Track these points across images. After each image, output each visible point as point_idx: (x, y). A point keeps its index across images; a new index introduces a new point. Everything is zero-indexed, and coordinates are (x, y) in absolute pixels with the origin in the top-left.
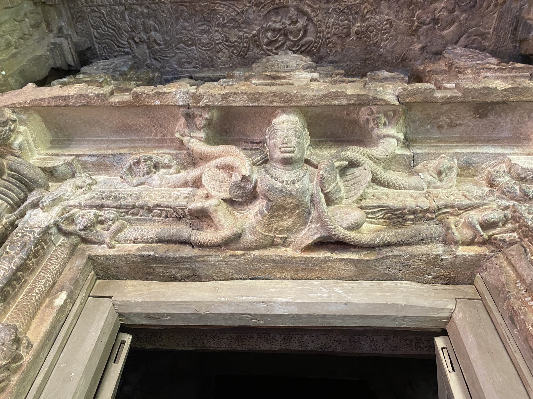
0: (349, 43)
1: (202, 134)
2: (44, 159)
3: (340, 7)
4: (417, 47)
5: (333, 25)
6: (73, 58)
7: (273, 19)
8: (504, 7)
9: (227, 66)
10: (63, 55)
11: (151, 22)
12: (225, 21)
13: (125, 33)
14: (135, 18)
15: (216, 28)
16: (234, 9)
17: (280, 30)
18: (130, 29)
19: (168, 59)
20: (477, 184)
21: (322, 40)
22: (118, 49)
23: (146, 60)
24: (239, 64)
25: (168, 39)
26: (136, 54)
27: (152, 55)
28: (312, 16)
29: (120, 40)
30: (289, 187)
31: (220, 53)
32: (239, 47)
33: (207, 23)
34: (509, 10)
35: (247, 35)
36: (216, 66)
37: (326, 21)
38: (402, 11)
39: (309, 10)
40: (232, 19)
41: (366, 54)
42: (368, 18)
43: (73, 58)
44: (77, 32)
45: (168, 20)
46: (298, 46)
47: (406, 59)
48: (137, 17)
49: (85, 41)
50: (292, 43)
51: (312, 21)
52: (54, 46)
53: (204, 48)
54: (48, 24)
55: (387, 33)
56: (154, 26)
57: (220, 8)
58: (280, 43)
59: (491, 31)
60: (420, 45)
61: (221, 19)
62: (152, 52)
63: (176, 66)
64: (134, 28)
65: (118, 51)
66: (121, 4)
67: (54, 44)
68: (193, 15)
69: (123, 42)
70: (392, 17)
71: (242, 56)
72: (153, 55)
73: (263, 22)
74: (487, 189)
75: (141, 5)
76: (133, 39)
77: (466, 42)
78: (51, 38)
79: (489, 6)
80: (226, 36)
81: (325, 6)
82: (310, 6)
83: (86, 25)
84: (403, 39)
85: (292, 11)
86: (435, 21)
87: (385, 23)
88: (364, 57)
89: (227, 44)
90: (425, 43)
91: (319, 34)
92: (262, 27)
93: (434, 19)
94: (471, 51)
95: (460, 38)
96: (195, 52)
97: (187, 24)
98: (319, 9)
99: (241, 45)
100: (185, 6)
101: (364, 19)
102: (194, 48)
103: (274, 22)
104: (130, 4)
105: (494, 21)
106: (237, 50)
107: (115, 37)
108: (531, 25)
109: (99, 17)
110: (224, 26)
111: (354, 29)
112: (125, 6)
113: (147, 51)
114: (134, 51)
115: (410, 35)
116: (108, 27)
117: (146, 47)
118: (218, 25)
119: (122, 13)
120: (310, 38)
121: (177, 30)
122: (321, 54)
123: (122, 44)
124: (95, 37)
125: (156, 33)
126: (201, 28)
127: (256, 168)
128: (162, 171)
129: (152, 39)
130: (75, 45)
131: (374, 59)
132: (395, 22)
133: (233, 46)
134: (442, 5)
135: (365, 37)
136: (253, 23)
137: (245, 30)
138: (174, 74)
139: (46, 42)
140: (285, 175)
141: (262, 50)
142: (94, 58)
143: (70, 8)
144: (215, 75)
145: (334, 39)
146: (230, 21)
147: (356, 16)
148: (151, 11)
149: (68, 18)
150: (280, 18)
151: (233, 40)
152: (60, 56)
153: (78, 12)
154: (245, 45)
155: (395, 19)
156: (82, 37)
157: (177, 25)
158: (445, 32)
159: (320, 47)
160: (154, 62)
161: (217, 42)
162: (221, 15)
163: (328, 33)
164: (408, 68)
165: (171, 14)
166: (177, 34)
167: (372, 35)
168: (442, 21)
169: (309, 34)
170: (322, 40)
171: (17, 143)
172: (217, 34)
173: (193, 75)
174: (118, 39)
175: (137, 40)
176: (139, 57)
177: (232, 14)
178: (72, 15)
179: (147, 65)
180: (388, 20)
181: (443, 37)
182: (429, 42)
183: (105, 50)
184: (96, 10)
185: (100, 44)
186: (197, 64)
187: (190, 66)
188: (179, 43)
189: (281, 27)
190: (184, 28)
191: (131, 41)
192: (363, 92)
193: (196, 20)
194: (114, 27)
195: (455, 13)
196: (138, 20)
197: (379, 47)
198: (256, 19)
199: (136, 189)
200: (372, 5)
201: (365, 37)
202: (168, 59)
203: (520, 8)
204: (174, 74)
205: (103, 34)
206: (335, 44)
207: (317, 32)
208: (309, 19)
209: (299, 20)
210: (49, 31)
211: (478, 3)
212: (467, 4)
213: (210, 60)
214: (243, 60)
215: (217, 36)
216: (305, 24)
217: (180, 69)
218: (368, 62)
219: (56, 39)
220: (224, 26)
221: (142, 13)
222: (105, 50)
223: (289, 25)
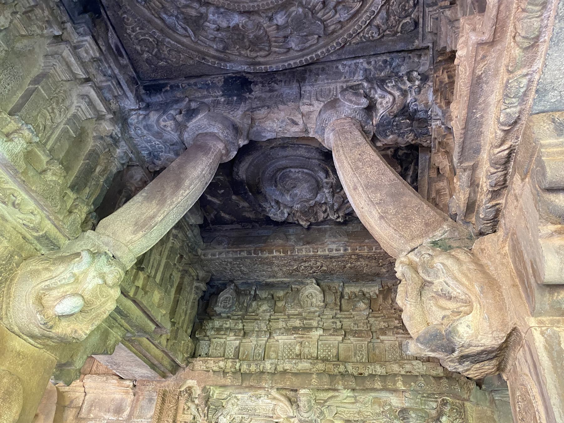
1: (275, 390)
2: (220, 393)
4: (384, 270)
20: (379, 406)
30: (307, 419)
74: (382, 409)
101: (351, 263)
120: (324, 268)
127: (295, 411)
128: (262, 398)
140: (306, 415)
171: (211, 393)
192: (331, 387)
199: (254, 404)
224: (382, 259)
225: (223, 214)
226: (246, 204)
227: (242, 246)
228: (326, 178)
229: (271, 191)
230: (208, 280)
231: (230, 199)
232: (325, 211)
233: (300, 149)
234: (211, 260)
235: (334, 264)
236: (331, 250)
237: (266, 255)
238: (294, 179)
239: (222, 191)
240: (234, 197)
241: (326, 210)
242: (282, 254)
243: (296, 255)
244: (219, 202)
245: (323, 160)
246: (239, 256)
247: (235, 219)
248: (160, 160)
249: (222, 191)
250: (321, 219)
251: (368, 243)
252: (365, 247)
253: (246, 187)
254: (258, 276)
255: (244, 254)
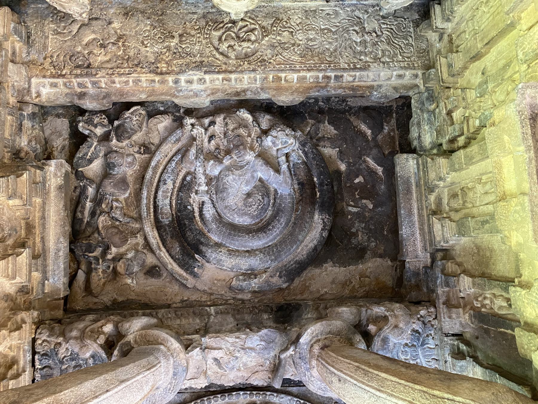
0: (180, 29)
3: (190, 58)
4: (116, 25)
5: (195, 44)
6: (434, 11)
7: (249, 50)
8: (44, 55)
9: (293, 11)
10: (443, 11)
11: (359, 49)
12: (292, 48)
13: (384, 40)
14: (373, 51)
15: (301, 43)
16: (284, 57)
17: (243, 41)
18: (379, 43)
19: (347, 18)
21: (204, 32)
22: (393, 27)
23: (368, 17)
24: (281, 13)
25: (345, 35)
26: (376, 22)
27: (362, 21)
28: (215, 51)
29: (389, 34)
31: (298, 22)
32: (281, 27)
33: (309, 47)
34: (39, 52)
35: (273, 37)
36: (303, 12)
37: (201, 47)
38: (135, 54)
39: (218, 56)
40: (286, 50)
41: (163, 20)
42: (164, 48)
43: (434, 11)
44: (428, 41)
45: (343, 50)
46: (226, 27)
47: (124, 15)
48: (371, 53)
49: (420, 31)
50: (232, 30)
51: (214, 47)
52: (448, 18)
53: (313, 26)
54: (451, 41)
55: (146, 37)
56: (357, 45)
57: (297, 58)
58: (243, 30)
59: (50, 37)
60: (113, 26)
61: (296, 50)
62: (362, 24)
63: (341, 12)
64: (375, 44)
65: (393, 25)
66: (384, 63)
67: (448, 20)
68: (321, 54)
69: (387, 33)
70: (143, 49)
71: (279, 20)
72: (361, 22)
73: (259, 47)
75: (366, 62)
76: (377, 36)
77: (71, 28)
78: (449, 26)
79: (58, 56)
80: (293, 36)
81: (203, 59)
82: (217, 59)
83: (418, 47)
84: (130, 31)
85: (232, 55)
86: (103, 46)
87: (148, 45)
88: (164, 17)
89: (292, 30)
90: (108, 27)
91: (208, 36)
92: (259, 43)
93: (105, 47)
94: (64, 9)
95: (78, 32)
96: (321, 23)
97: (327, 47)
98: (208, 57)
99: (279, 28)
100: (327, 60)
101: (168, 48)
102: (322, 27)
103: (248, 47)
104: (375, 62)
105: (50, 44)
106: (283, 24)
107: (393, 36)
108: (16, 34)
109: (404, 52)
110: (293, 45)
111: (176, 40)
112: (380, 61)
113: (366, 25)
114: (378, 25)
115: (124, 35)
116: (399, 45)
117: (367, 29)
118: (299, 45)
119: (383, 56)
120: (217, 34)
121: (337, 41)
122: (204, 21)
123: (388, 31)
124: (411, 37)
125: (356, 40)
126: (315, 43)
129: (360, 34)
130: (430, 26)
131: (154, 15)
132: (140, 46)
133: (286, 28)
134: (99, 58)
135: (165, 34)
136: (268, 46)
137: (275, 41)
138: (343, 4)
139: (456, 20)
141: (259, 25)
142: (416, 20)
143: (429, 60)
144: (305, 3)
145: (193, 32)
146: (289, 48)
147: (175, 51)
148: (358, 57)
149: (432, 52)
150: (244, 51)
151: (286, 33)
152: (445, 8)
153: (423, 57)
154: (275, 29)
155: (140, 48)
156: (423, 36)
157: (336, 46)
158: (93, 36)
159: (206, 25)
160: (361, 16)
161: (301, 31)
162: (296, 53)
163: (199, 37)
164: (121, 6)
165: (340, 54)
166: (336, 38)
167: (159, 35)
168: (97, 46)
169: (217, 38)
170: (204, 32)
172: (300, 38)
173: (326, 3)
174: (391, 35)
175: (374, 34)
176: (374, 20)
177: (286, 54)
178: (428, 55)
179: (368, 13)
180: (146, 47)
181: (94, 32)
182: (105, 28)
183: (404, 26)
184: (406, 59)
185: (409, 31)
186: (321, 13)
187: (327, 12)
188: (336, 31)
189: (242, 43)
190: (330, 43)
191: (379, 33)
193: (318, 49)
194: (393, 45)
195: (87, 52)
196: (370, 50)
197: (152, 25)
198: (265, 49)
200: (162, 59)
201: (165, 34)
202: (347, 18)
203: (29, 54)
204: (343, 4)
205: (404, 39)
206: (192, 28)
207: (209, 38)
208: (217, 49)
209: (226, 49)
210: (451, 35)
211: (68, 59)
212: (78, 58)
213: (308, 17)
214: (277, 16)
215: (300, 36)
216: (221, 45)
217: (337, 9)
218: (160, 13)
219: (446, 27)
220: (293, 45)
221: (366, 55)
222: (404, 26)
223: (235, 45)
224: (118, 57)
225: (369, 132)
226: (329, 151)
227: (348, 92)
228: (203, 202)
229: (283, 185)
230: (423, 25)
231: (349, 165)
232: (211, 138)
233: (230, 266)
234: (405, 68)
235: (197, 47)
236: (201, 81)
237: (309, 75)
238: (245, 214)
239: (357, 181)
240: (343, 167)
241: (209, 141)
242: (283, 75)
243: (258, 74)
244: (368, 159)
245: (202, 243)
246: (358, 74)
247: (352, 119)
248: (414, 331)
249: (357, 181)
250: (219, 119)
251: (141, 92)
252: (145, 85)
253: (318, 194)
254: (336, 13)
255: (347, 77)
